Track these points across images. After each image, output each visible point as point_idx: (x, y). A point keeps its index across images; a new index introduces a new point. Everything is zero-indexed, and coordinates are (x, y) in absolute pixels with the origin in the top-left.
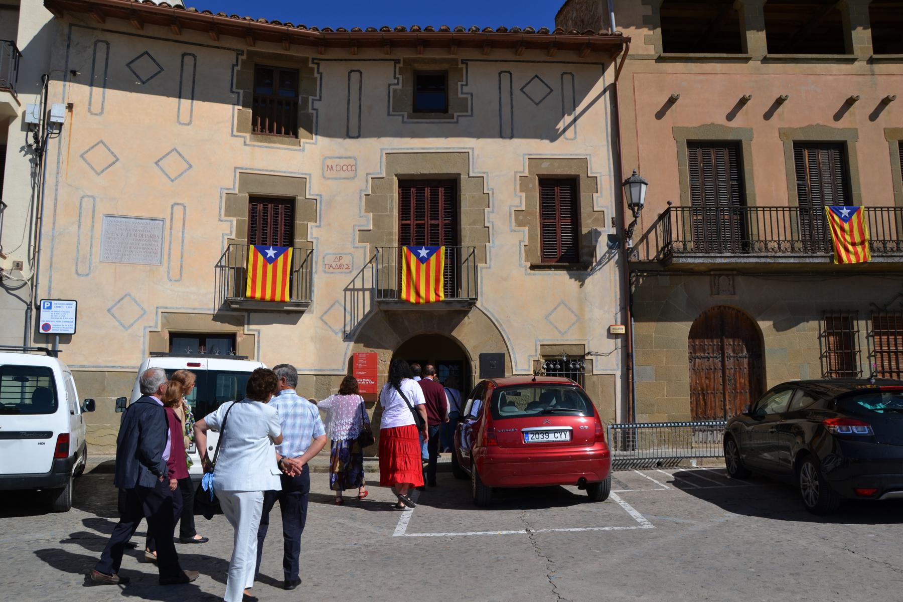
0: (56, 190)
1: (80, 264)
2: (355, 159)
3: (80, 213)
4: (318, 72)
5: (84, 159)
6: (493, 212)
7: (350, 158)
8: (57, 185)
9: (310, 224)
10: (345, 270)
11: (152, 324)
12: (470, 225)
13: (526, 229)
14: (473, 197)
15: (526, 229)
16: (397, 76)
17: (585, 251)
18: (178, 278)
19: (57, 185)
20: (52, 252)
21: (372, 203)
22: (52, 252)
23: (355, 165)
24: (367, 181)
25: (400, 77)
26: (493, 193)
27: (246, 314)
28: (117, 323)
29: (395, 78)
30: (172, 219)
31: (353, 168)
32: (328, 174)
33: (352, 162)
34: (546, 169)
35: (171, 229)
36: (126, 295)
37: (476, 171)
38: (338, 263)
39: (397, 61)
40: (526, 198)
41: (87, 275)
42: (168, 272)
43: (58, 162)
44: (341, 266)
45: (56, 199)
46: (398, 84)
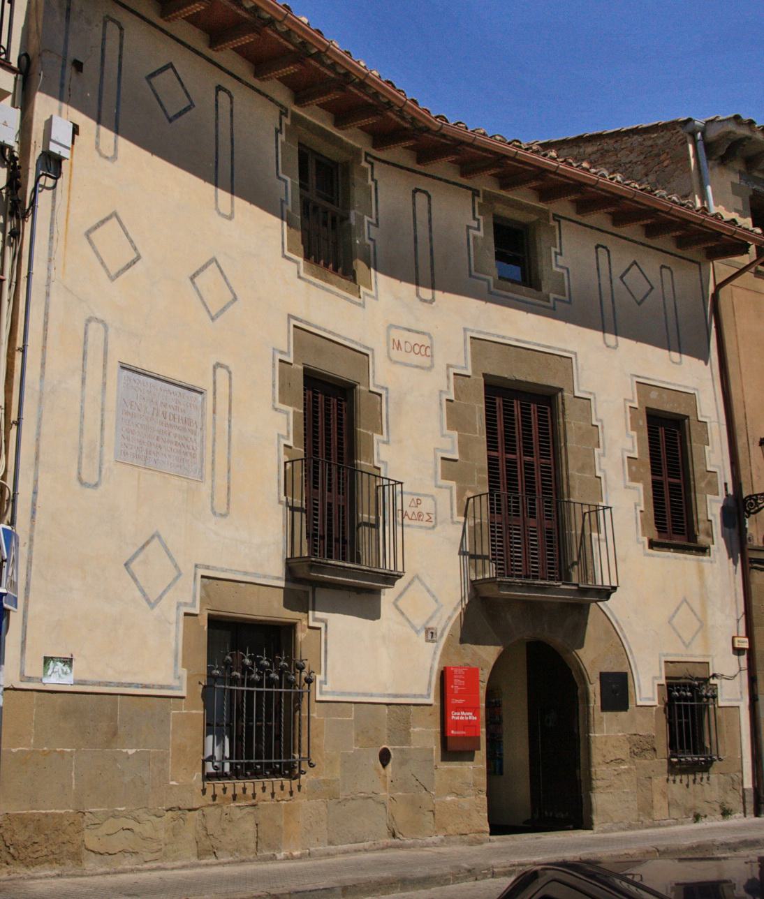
0: (48, 294)
1: (84, 461)
2: (431, 338)
3: (85, 353)
4: (373, 180)
5: (632, 265)
6: (604, 455)
7: (423, 333)
8: (48, 285)
9: (376, 437)
10: (424, 524)
11: (189, 600)
12: (578, 471)
13: (640, 486)
14: (580, 428)
15: (640, 486)
16: (477, 216)
17: (702, 526)
18: (224, 511)
19: (48, 285)
20: (39, 427)
21: (455, 416)
22: (39, 427)
23: (431, 347)
24: (448, 377)
25: (481, 218)
26: (603, 427)
27: (309, 589)
28: (138, 594)
29: (474, 218)
30: (214, 393)
31: (427, 350)
32: (395, 354)
33: (425, 341)
34: (657, 402)
35: (214, 412)
36: (153, 537)
37: (582, 388)
38: (416, 510)
39: (475, 193)
40: (638, 439)
41: (96, 485)
42: (213, 499)
43: (51, 238)
44: (420, 514)
45: (46, 314)
46: (478, 229)
